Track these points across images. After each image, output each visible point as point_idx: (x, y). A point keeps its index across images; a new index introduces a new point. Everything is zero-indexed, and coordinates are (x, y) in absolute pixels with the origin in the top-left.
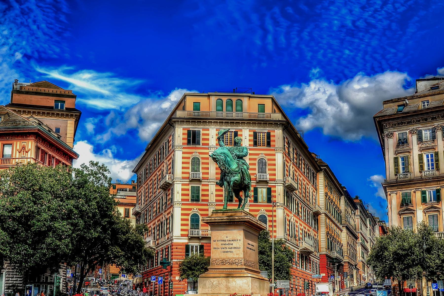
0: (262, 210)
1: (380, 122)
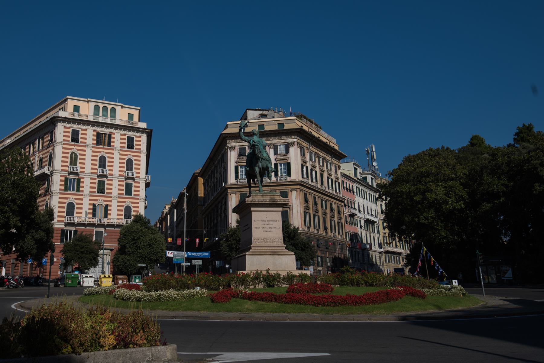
0: (128, 202)
1: (224, 138)
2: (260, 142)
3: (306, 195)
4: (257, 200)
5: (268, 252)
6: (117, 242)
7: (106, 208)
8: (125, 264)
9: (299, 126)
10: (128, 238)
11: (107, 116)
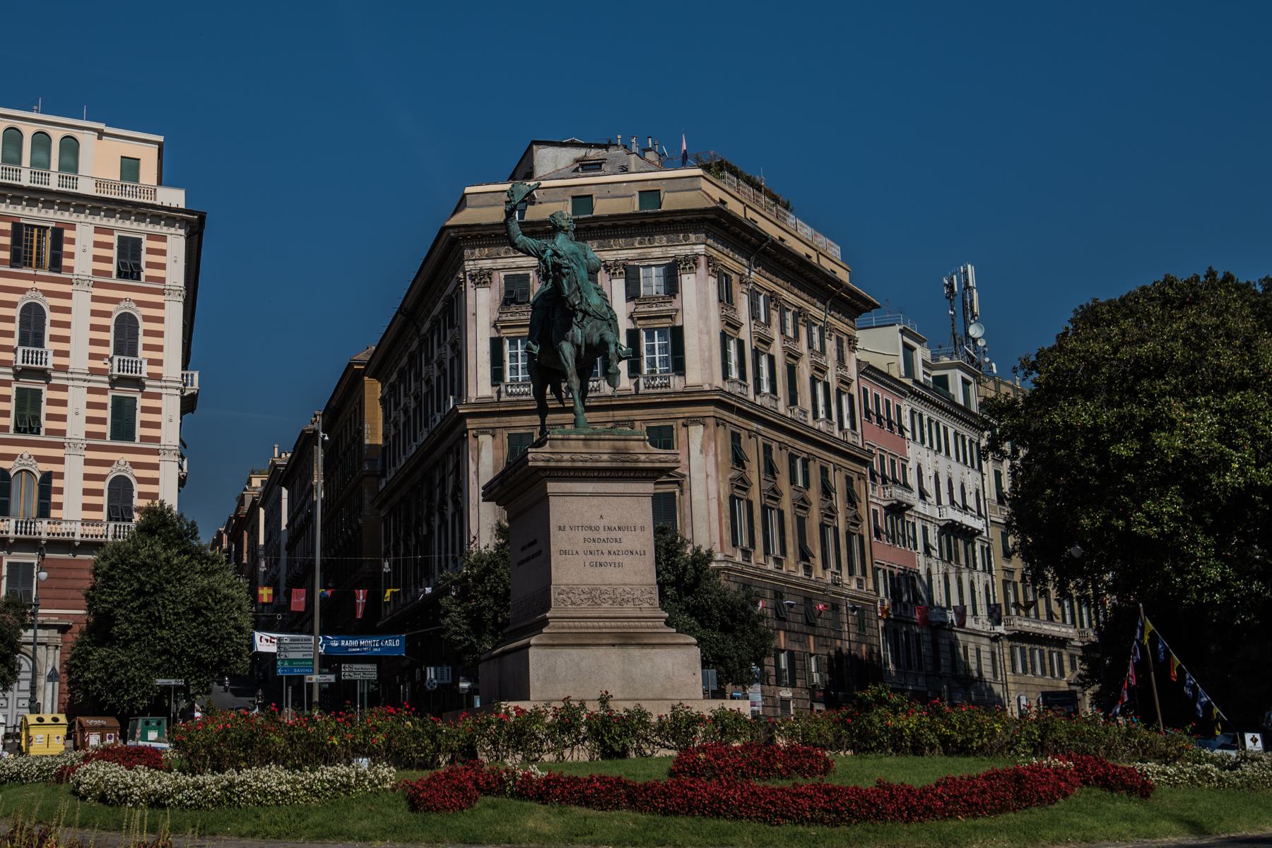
0: (122, 462)
1: (454, 242)
2: (576, 254)
3: (735, 437)
4: (566, 457)
5: (607, 635)
6: (84, 603)
7: (46, 486)
8: (110, 678)
9: (714, 201)
10: (121, 589)
11: (48, 167)
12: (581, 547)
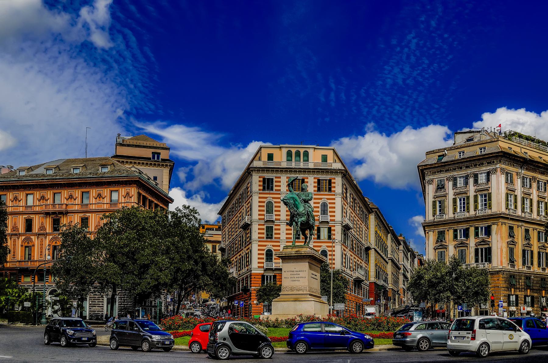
0: (324, 246)
12: (290, 276)
